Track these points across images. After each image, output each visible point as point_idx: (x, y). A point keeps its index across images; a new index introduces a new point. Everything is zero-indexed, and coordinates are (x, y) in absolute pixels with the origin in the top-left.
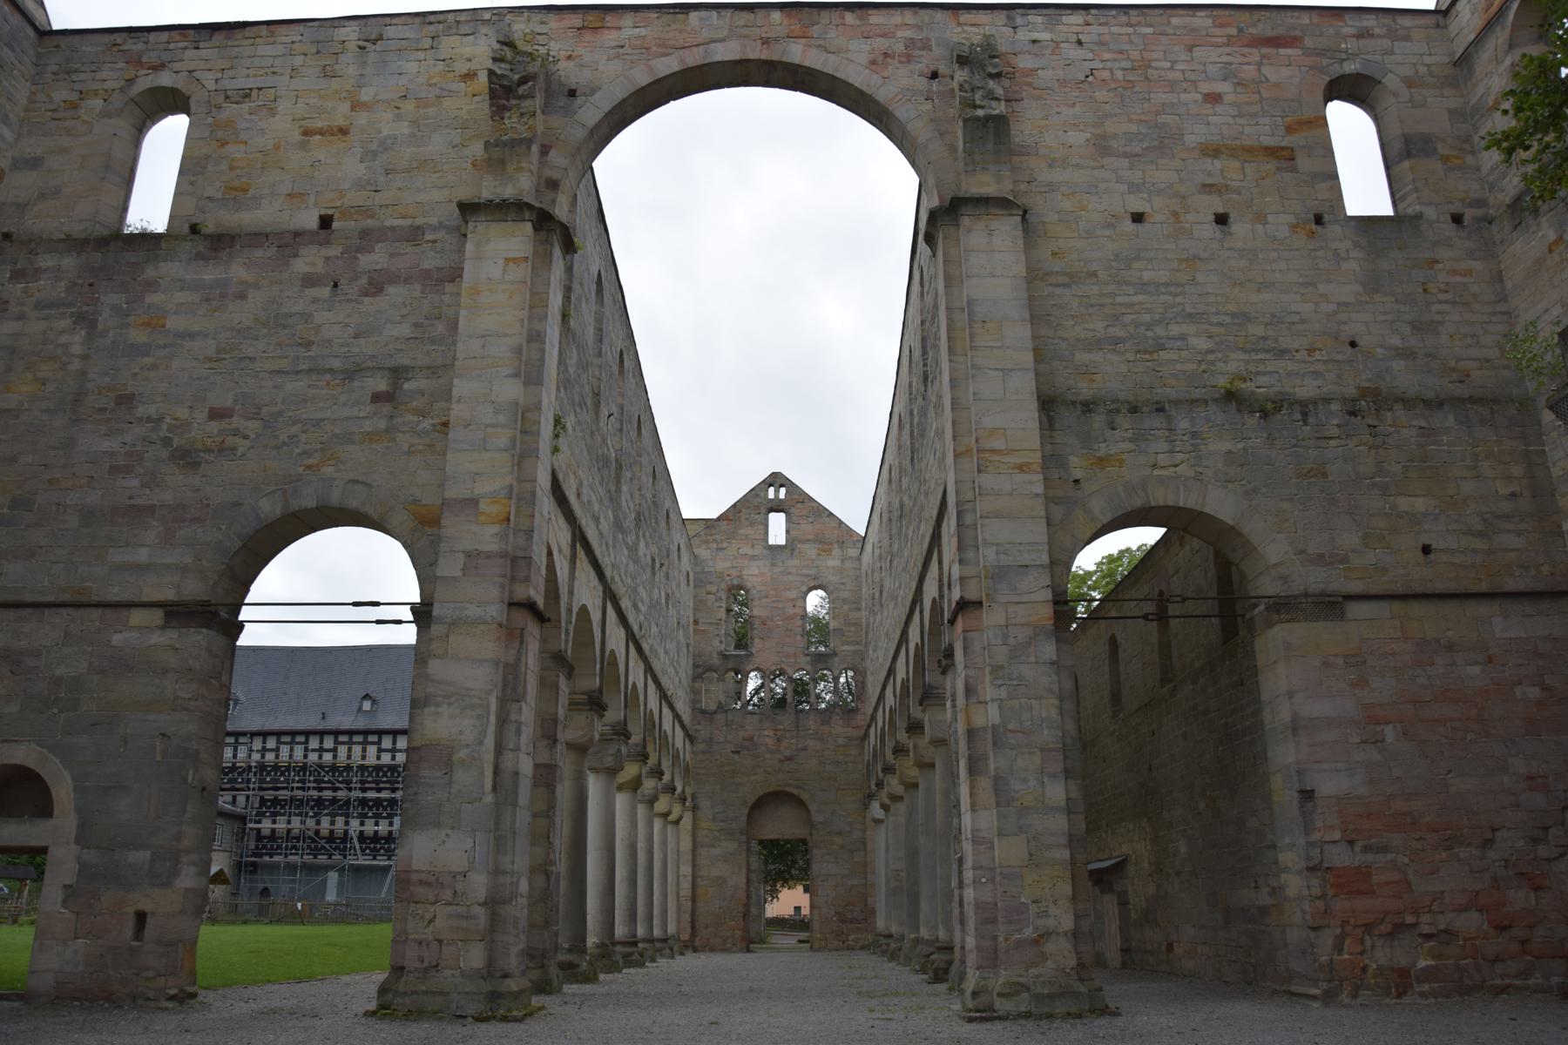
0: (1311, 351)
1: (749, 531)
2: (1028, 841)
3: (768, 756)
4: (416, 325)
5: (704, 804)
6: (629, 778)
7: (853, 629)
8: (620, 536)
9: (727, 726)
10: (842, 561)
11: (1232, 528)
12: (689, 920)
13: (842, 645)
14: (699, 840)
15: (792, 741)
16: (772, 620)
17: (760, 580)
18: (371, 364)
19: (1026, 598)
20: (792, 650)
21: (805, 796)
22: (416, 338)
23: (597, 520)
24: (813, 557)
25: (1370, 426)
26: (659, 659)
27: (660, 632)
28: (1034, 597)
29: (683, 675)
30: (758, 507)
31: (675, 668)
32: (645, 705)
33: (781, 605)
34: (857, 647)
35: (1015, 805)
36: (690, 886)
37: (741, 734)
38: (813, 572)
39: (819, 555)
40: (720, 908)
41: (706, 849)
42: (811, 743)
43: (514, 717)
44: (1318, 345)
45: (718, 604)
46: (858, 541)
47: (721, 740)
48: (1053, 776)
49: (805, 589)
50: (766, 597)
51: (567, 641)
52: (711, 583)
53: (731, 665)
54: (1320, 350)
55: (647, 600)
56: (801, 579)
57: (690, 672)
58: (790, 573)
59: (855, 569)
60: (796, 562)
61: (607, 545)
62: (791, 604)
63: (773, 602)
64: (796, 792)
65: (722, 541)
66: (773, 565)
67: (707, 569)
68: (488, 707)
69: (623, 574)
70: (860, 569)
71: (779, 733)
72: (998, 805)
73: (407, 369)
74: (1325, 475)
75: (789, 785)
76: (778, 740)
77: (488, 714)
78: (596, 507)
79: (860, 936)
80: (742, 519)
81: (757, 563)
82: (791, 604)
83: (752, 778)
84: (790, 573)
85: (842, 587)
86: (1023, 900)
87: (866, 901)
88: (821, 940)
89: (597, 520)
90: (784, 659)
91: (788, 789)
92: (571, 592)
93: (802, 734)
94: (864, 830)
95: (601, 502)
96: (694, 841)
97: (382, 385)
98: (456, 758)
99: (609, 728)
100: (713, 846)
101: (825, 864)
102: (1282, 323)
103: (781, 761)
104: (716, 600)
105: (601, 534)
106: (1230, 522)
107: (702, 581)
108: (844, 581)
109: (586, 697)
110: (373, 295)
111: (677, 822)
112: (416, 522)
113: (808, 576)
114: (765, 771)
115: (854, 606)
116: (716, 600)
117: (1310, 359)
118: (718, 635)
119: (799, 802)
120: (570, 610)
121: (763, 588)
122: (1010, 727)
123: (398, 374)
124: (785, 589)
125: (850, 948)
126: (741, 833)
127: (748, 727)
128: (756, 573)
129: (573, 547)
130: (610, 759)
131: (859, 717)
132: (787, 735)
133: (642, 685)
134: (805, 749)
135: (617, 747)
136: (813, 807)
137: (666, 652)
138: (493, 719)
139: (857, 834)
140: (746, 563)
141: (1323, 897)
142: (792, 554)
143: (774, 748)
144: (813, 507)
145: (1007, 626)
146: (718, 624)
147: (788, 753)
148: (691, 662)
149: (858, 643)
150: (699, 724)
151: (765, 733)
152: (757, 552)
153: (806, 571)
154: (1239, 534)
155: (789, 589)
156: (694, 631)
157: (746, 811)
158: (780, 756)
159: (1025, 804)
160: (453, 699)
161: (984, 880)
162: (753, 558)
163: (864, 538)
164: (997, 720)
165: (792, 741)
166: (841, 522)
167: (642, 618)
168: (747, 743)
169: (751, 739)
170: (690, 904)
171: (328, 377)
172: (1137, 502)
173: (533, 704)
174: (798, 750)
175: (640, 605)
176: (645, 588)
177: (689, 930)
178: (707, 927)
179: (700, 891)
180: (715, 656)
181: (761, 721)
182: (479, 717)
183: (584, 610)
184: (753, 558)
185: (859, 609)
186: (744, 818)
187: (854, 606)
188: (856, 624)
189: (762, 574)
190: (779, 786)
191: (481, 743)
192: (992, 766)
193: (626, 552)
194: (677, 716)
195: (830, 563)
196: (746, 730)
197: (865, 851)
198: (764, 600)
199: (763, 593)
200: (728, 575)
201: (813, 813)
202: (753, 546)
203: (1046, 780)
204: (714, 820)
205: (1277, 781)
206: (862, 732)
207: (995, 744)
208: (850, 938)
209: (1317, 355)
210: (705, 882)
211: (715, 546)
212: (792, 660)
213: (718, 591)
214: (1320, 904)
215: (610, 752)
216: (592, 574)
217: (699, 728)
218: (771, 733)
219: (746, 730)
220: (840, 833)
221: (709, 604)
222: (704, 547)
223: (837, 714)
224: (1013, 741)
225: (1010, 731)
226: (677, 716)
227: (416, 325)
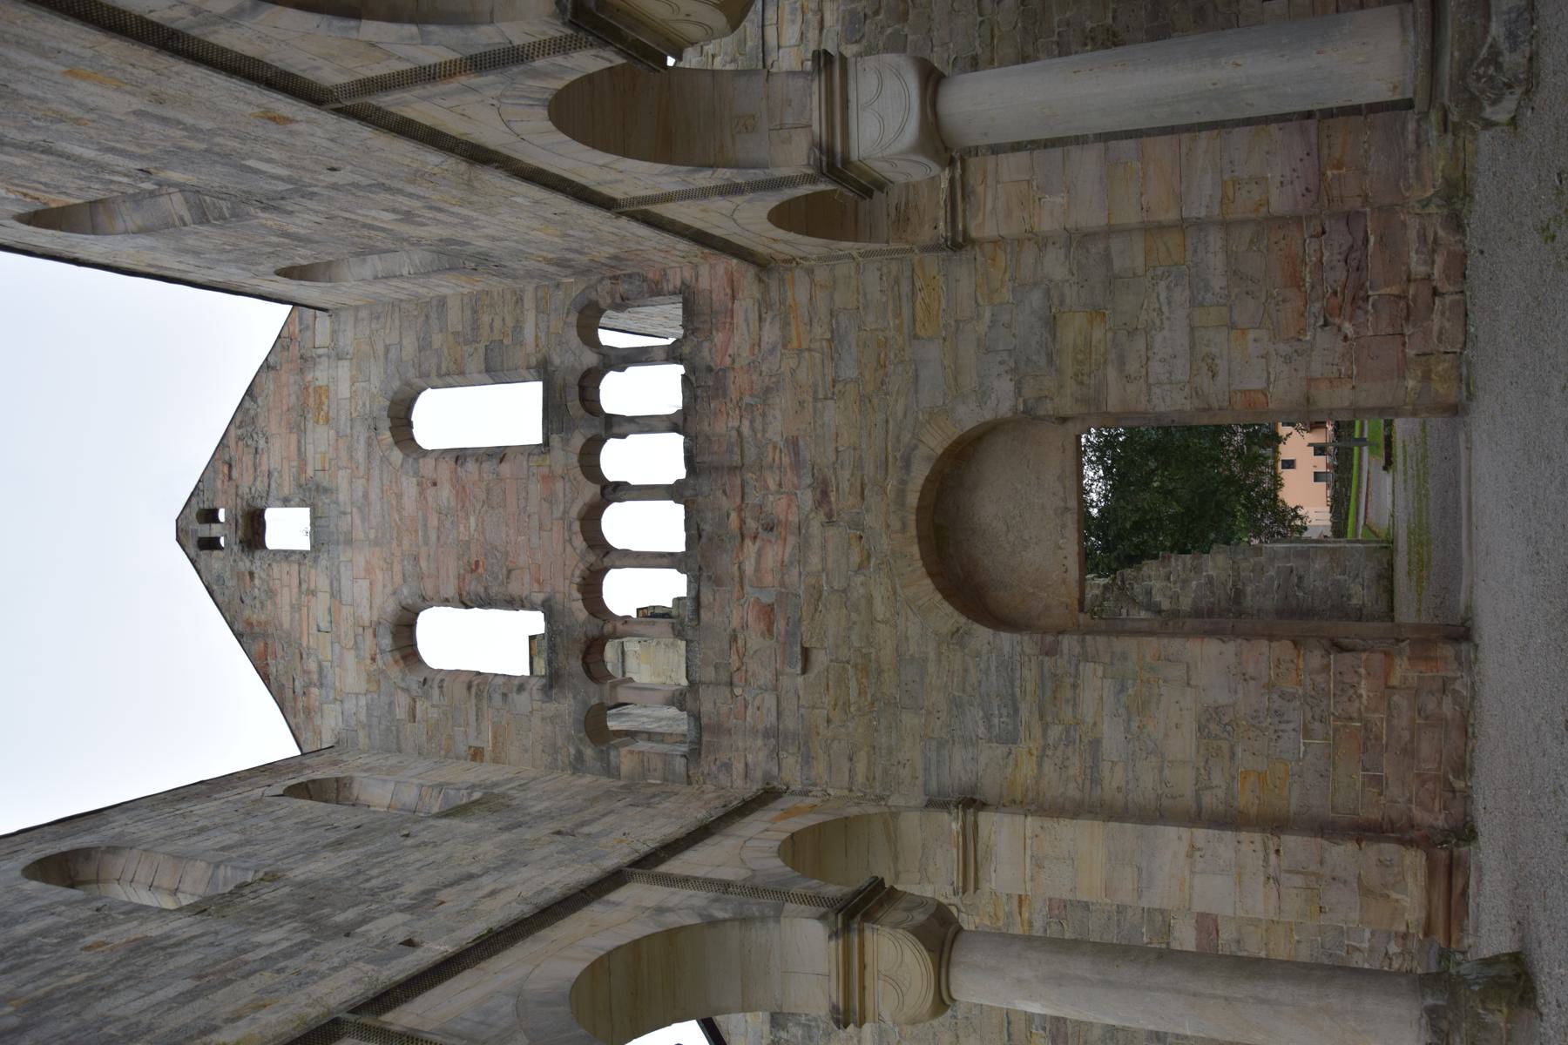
1: (285, 598)
3: (815, 562)
5: (960, 769)
7: (486, 319)
10: (339, 358)
12: (1351, 847)
13: (521, 343)
14: (1073, 791)
15: (772, 485)
16: (467, 544)
17: (379, 576)
20: (536, 488)
21: (936, 442)
24: (332, 433)
30: (240, 576)
33: (434, 522)
34: (529, 303)
36: (1229, 835)
37: (754, 640)
38: (362, 433)
39: (327, 420)
40: (1307, 733)
41: (1105, 767)
42: (777, 428)
45: (436, 692)
46: (301, 319)
47: (770, 701)
49: (397, 455)
50: (416, 558)
52: (391, 704)
53: (576, 665)
56: (376, 472)
58: (366, 496)
59: (356, 320)
60: (343, 477)
62: (431, 491)
63: (426, 543)
64: (920, 473)
65: (306, 672)
66: (349, 542)
67: (363, 717)
70: (357, 308)
71: (751, 524)
75: (901, 493)
76: (769, 528)
79: (1412, 234)
80: (263, 618)
81: (345, 583)
82: (431, 491)
83: (880, 610)
84: (366, 496)
85: (393, 354)
87: (1282, 221)
88: (1426, 377)
90: (558, 513)
91: (913, 499)
93: (751, 453)
94: (1041, 242)
96: (1077, 811)
100: (1096, 743)
101: (1156, 367)
103: (829, 515)
104: (427, 696)
107: (388, 729)
108: (380, 349)
113: (369, 445)
114: (860, 567)
115: (434, 315)
116: (427, 696)
118: (505, 695)
121: (397, 568)
124: (400, 509)
125: (1459, 268)
126: (1051, 652)
127: (735, 622)
128: (365, 584)
131: (704, 283)
132: (754, 498)
134: (793, 444)
136: (969, 417)
139: (1055, 266)
140: (345, 610)
142: (326, 490)
143: (792, 540)
144: (240, 438)
147: (807, 498)
149: (519, 301)
150: (727, 767)
151: (749, 568)
152: (320, 580)
153: (360, 455)
155: (399, 496)
156: (496, 760)
157: (982, 634)
158: (815, 527)
162: (335, 594)
163: (295, 304)
165: (772, 485)
166: (266, 366)
168: (780, 625)
169: (768, 612)
170: (1291, 842)
174: (797, 465)
177: (1390, 849)
178: (1378, 781)
179: (1247, 799)
180: (551, 708)
181: (717, 582)
184: (335, 594)
185: (442, 302)
186: (1006, 639)
187: (434, 315)
188: (475, 312)
189: (369, 570)
190: (904, 528)
195: (344, 390)
196: (745, 627)
197: (1111, 231)
198: (424, 564)
199: (409, 568)
200: (373, 659)
201: (988, 416)
202: (312, 593)
204: (1010, 739)
206: (747, 276)
208: (1418, 268)
210: (1218, 779)
211: (315, 691)
213: (407, 690)
217: (738, 767)
218: (751, 548)
219: (745, 627)
220: (1051, 323)
221: (434, 714)
222: (318, 722)
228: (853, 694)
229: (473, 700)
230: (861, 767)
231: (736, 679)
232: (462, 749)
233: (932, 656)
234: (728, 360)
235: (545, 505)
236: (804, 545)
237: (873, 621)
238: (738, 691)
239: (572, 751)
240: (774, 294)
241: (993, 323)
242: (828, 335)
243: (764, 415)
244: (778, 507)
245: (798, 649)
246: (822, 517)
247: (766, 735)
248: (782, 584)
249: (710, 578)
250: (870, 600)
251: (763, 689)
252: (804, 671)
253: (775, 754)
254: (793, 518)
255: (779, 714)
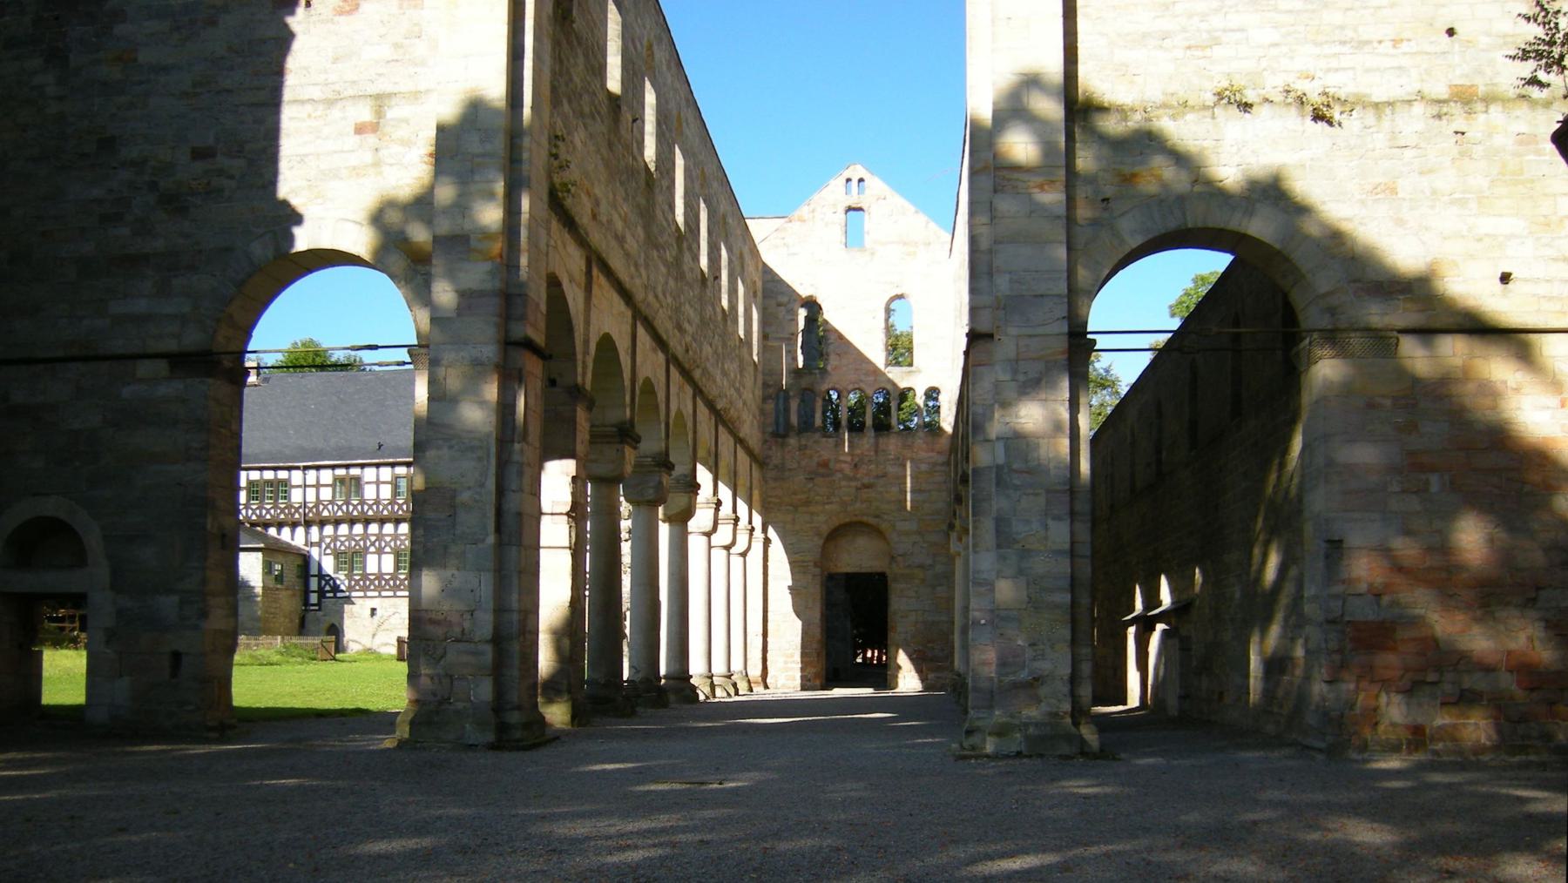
0: (1396, 42)
2: (1028, 584)
3: (844, 483)
4: (397, 46)
6: (678, 510)
8: (655, 254)
9: (800, 450)
11: (1279, 253)
15: (870, 467)
18: (351, 92)
19: (1040, 331)
21: (884, 526)
22: (397, 61)
23: (620, 240)
25: (1456, 133)
26: (715, 381)
27: (715, 352)
28: (1048, 330)
29: (747, 395)
31: (737, 390)
32: (695, 432)
35: (1016, 546)
43: (516, 457)
44: (1405, 35)
45: (790, 317)
47: (795, 466)
48: (1058, 518)
51: (584, 374)
54: (1409, 40)
55: (697, 320)
57: (759, 393)
61: (636, 266)
68: (488, 450)
69: (661, 296)
72: (999, 546)
73: (390, 95)
74: (1394, 191)
76: (856, 466)
77: (488, 456)
78: (619, 225)
86: (1020, 642)
89: (620, 240)
90: (863, 377)
91: (865, 519)
92: (587, 322)
95: (625, 220)
97: (365, 114)
98: (459, 499)
99: (649, 459)
102: (1366, 8)
103: (858, 489)
105: (627, 255)
106: (1277, 246)
109: (615, 429)
110: (350, 12)
111: (744, 555)
112: (409, 261)
117: (1394, 51)
119: (876, 532)
120: (586, 342)
122: (1015, 466)
123: (380, 101)
129: (589, 273)
130: (651, 491)
133: (691, 412)
134: (884, 476)
135: (658, 478)
137: (725, 374)
138: (493, 461)
141: (1340, 651)
143: (852, 474)
145: (1017, 361)
146: (789, 339)
147: (866, 481)
148: (760, 382)
154: (1286, 259)
157: (821, 542)
159: (1027, 546)
160: (454, 442)
161: (983, 622)
164: (1001, 459)
167: (688, 339)
168: (822, 470)
169: (825, 464)
171: (309, 108)
172: (1172, 224)
173: (537, 444)
174: (877, 477)
175: (686, 326)
176: (691, 306)
182: (480, 459)
183: (607, 343)
190: (856, 515)
191: (482, 485)
192: (995, 508)
193: (663, 270)
194: (740, 441)
203: (1050, 522)
205: (1309, 528)
207: (998, 484)
209: (1405, 47)
212: (872, 378)
214: (1337, 657)
215: (652, 484)
216: (616, 298)
220: (921, 566)
223: (920, 439)
224: (1017, 482)
225: (1016, 471)
226: (740, 441)
227: (397, 46)
228: (799, 497)
229: (787, 336)
230: (773, 500)
231: (802, 452)
232: (768, 330)
233: (813, 525)
234: (915, 450)
235: (864, 371)
236: (850, 479)
237: (825, 504)
238: (797, 453)
239: (771, 383)
240: (938, 468)
241: (922, 547)
242: (922, 489)
243: (895, 464)
244: (863, 470)
245: (813, 476)
246: (859, 486)
247: (783, 464)
248: (837, 471)
249: (837, 441)
250: (831, 503)
251: (799, 463)
252: (806, 479)
253: (776, 466)
254: (859, 476)
255: (790, 470)
